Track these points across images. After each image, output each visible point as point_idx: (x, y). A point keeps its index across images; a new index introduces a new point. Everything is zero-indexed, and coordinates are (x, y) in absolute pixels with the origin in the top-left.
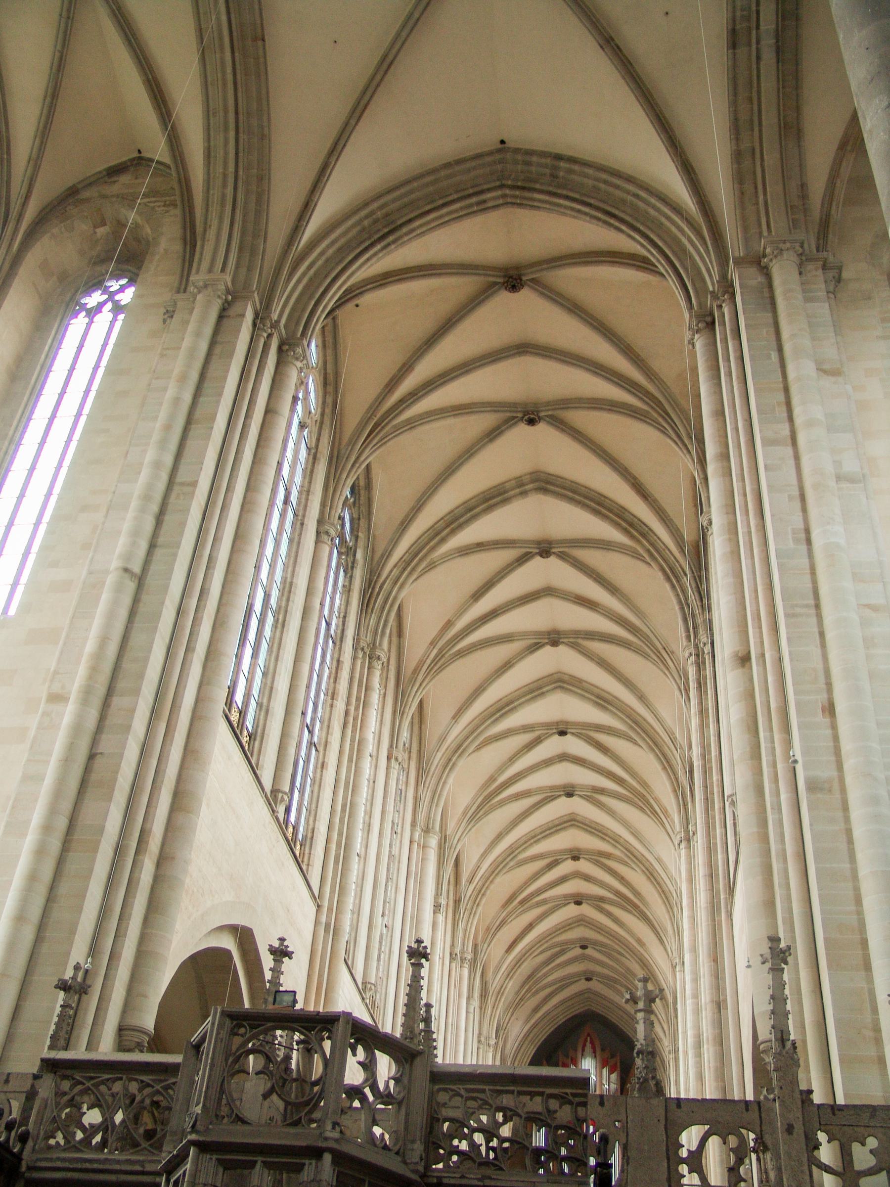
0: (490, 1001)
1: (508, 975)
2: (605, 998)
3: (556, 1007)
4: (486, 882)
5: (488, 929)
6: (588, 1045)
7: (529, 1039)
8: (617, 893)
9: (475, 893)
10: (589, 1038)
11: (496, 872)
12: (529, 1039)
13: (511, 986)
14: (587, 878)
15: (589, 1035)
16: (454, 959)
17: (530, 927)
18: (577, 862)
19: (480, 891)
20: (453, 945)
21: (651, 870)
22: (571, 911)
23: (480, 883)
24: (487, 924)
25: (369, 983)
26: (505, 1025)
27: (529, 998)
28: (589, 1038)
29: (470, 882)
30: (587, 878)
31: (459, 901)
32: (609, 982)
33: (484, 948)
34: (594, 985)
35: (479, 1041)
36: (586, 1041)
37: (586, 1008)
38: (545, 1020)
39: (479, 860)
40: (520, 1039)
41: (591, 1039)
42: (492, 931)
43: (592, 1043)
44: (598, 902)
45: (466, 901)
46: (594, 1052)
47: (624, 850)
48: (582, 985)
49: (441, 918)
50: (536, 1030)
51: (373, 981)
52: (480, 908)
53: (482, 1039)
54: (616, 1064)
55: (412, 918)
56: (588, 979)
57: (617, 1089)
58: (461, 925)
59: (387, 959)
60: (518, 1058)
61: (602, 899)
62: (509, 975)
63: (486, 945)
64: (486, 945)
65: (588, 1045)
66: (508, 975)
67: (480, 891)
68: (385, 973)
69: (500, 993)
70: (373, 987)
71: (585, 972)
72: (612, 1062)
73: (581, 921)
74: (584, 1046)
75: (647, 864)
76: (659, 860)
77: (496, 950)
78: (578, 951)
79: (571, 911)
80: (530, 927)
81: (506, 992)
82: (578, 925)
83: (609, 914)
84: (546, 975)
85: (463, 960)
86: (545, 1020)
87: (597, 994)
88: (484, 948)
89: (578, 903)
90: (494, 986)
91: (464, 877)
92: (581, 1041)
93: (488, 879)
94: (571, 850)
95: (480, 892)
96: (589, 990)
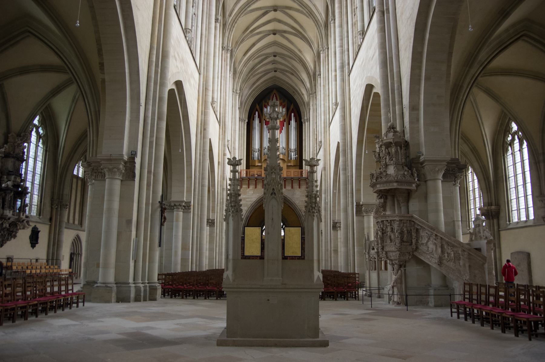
0: (238, 75)
1: (244, 66)
2: (281, 79)
3: (262, 83)
4: (237, 17)
5: (237, 42)
6: (275, 97)
7: (251, 95)
8: (293, 28)
9: (232, 21)
11: (242, 12)
13: (245, 70)
14: (280, 21)
15: (275, 94)
16: (224, 49)
17: (254, 45)
18: (276, 12)
19: (234, 21)
20: (223, 43)
21: (310, 11)
22: (271, 38)
23: (234, 17)
24: (236, 40)
25: (188, 29)
27: (252, 78)
29: (230, 16)
30: (280, 21)
31: (225, 24)
32: (283, 71)
33: (236, 50)
34: (278, 74)
35: (233, 91)
36: (274, 96)
38: (257, 88)
39: (234, 6)
40: (248, 95)
42: (238, 43)
43: (276, 96)
44: (282, 33)
45: (229, 24)
47: (299, 3)
48: (272, 74)
49: (218, 25)
51: (190, 28)
52: (234, 29)
53: (234, 90)
54: (285, 105)
55: (207, 13)
56: (275, 71)
57: (285, 114)
58: (227, 35)
59: (195, 29)
60: (247, 103)
61: (285, 32)
62: (245, 65)
63: (236, 49)
64: (236, 49)
65: (275, 97)
66: (244, 66)
67: (234, 21)
68: (195, 35)
69: (241, 73)
70: (190, 31)
71: (274, 68)
72: (283, 104)
73: (275, 43)
74: (273, 97)
75: (309, 9)
76: (315, 6)
77: (239, 53)
78: (272, 58)
79: (271, 38)
80: (254, 45)
81: (244, 72)
82: (274, 45)
83: (287, 39)
84: (258, 69)
85: (227, 50)
86: (257, 88)
87: (279, 78)
88: (236, 50)
89: (274, 34)
90: (239, 69)
91: (227, 14)
92: (271, 97)
93: (238, 15)
94: (273, 7)
95: (234, 21)
96: (275, 76)
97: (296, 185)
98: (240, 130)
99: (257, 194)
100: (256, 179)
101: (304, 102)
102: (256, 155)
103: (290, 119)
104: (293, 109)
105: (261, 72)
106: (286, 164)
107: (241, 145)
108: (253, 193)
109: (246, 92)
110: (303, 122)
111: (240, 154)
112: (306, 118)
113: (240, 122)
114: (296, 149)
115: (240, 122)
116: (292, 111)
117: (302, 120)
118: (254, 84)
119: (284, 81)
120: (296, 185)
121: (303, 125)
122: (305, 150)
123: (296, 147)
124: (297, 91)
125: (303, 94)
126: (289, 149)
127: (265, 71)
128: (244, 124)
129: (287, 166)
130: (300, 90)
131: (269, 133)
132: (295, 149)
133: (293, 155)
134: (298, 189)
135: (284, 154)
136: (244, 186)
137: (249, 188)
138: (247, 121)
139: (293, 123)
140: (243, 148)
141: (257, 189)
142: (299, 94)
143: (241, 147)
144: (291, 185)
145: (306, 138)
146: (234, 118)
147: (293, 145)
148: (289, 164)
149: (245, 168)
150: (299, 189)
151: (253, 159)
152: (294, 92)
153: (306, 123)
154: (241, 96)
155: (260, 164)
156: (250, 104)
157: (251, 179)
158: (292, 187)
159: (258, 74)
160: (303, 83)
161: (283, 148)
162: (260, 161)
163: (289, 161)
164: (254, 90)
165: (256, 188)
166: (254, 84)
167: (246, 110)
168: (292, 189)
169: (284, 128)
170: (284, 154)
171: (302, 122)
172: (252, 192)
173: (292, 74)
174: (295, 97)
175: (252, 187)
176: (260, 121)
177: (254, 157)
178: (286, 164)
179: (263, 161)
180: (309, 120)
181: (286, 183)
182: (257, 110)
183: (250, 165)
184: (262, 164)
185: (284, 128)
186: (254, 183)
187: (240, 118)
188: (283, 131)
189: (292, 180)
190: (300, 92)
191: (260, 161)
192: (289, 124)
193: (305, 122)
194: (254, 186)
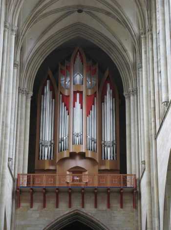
3: (57, 34)
6: (78, 56)
7: (40, 52)
10: (78, 53)
12: (40, 52)
15: (78, 51)
26: (23, 32)
28: (78, 53)
34: (85, 18)
35: (5, 26)
37: (77, 35)
41: (80, 53)
43: (80, 55)
46: (82, 61)
50: (43, 48)
56: (80, 11)
60: (32, 65)
65: (78, 56)
74: (75, 57)
97: (115, 204)
98: (20, 108)
99: (46, 219)
100: (45, 191)
101: (127, 64)
102: (46, 151)
103: (104, 94)
104: (108, 77)
105: (56, 11)
106: (97, 168)
107: (20, 133)
108: (40, 216)
109: (31, 47)
110: (126, 97)
111: (18, 148)
112: (131, 89)
113: (20, 96)
114: (115, 142)
115: (20, 96)
116: (108, 80)
117: (124, 94)
118: (44, 33)
119: (94, 30)
120: (115, 204)
121: (127, 101)
122: (130, 142)
123: (115, 139)
124: (114, 46)
125: (125, 51)
126: (103, 142)
127: (62, 9)
128: (27, 98)
129: (99, 170)
130: (121, 44)
131: (68, 114)
132: (113, 142)
133: (109, 151)
134: (119, 209)
135: (94, 151)
136: (24, 205)
137: (31, 207)
138: (31, 94)
139: (109, 104)
140: (23, 138)
141: (45, 209)
142: (118, 49)
143: (20, 136)
144: (106, 202)
145: (132, 121)
146: (6, 71)
147: (109, 136)
148: (103, 168)
149: (26, 172)
150: (121, 209)
151: (40, 157)
152: (110, 48)
153: (132, 98)
154: (20, 47)
155: (52, 168)
156: (38, 66)
157: (36, 192)
158: (109, 206)
159: (51, 13)
160: (127, 26)
161: (92, 140)
162: (52, 162)
163: (103, 161)
164: (43, 45)
165: (44, 206)
166: (44, 33)
167: (30, 77)
168: (109, 210)
169: (95, 108)
170: (94, 151)
171: (124, 97)
172: (38, 215)
173: (108, 14)
174: (113, 57)
175: (37, 205)
176: (54, 97)
177: (42, 156)
178: (97, 168)
179: (57, 161)
180: (136, 92)
181: (98, 198)
182: (49, 78)
183: (36, 168)
184: (56, 168)
185: (95, 108)
186: (42, 197)
187: (19, 87)
188: (92, 112)
189: (108, 192)
190: (120, 47)
191: (52, 162)
192: (102, 100)
193: (129, 97)
194: (41, 204)
